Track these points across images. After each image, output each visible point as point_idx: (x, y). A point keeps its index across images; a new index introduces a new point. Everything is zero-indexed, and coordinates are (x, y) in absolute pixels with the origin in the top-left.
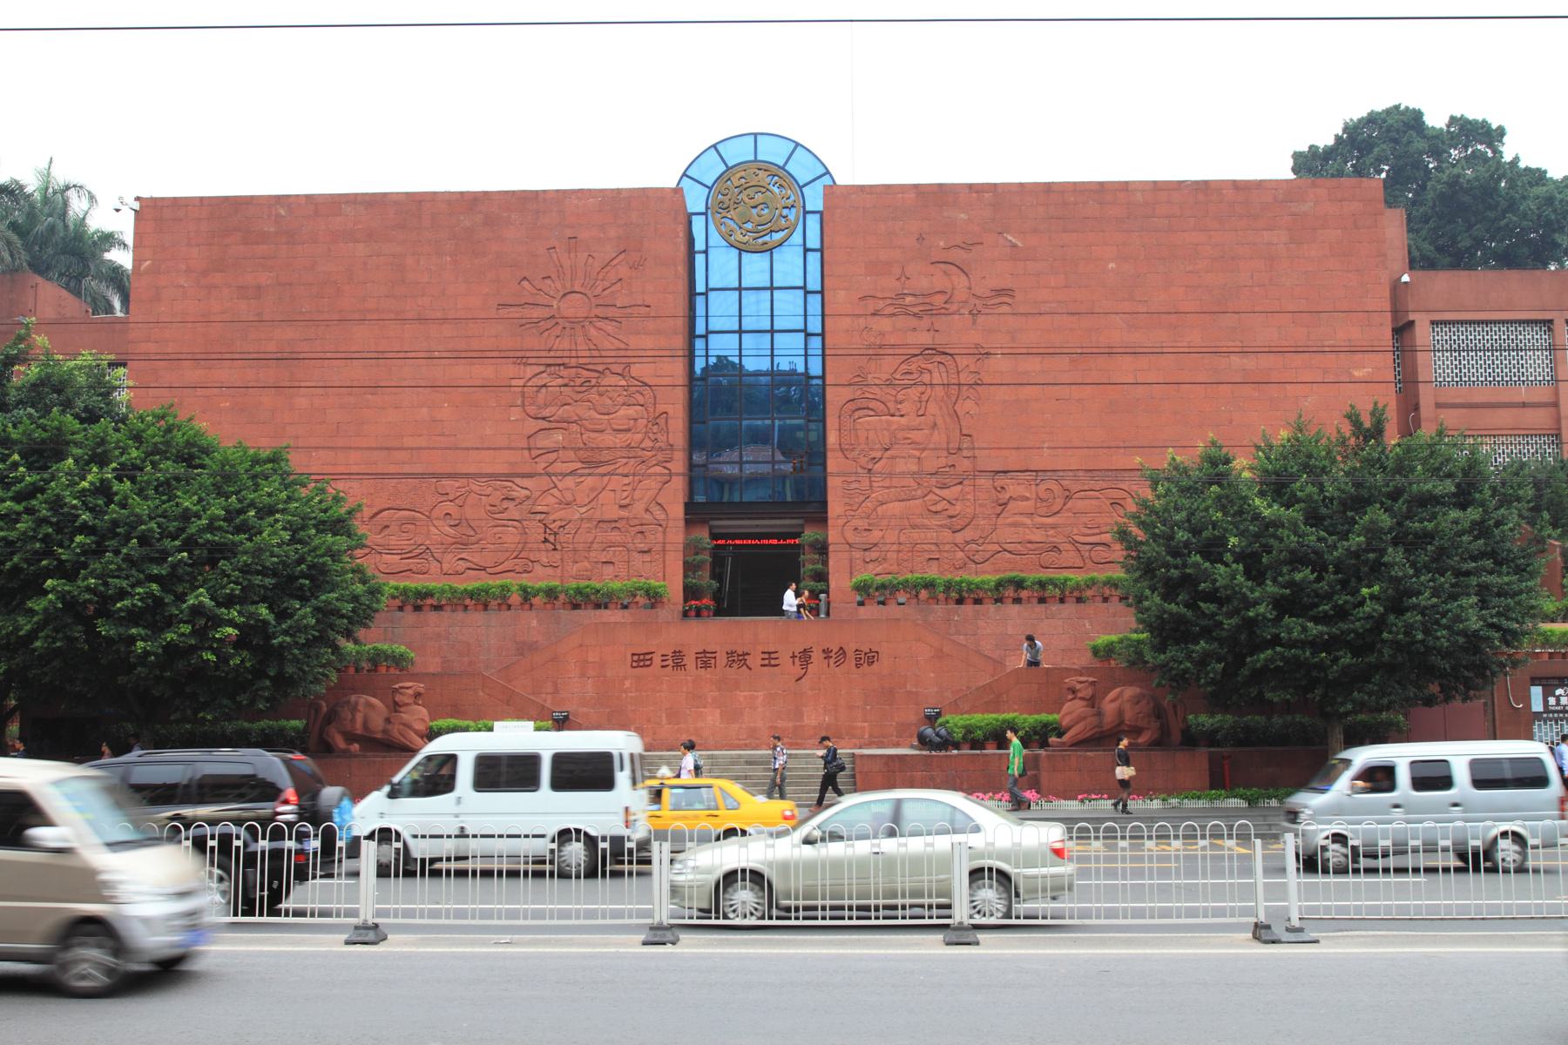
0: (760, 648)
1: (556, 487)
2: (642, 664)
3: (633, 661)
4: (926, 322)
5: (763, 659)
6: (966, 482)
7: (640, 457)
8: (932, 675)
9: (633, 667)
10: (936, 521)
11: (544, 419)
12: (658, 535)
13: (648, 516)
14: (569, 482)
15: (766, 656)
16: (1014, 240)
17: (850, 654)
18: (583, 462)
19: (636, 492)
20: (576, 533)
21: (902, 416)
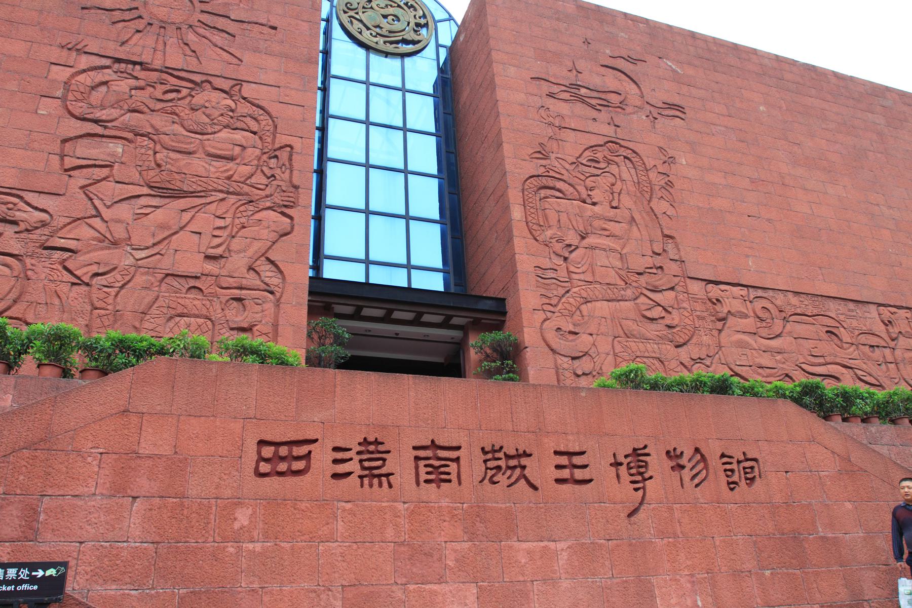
0: (551, 444)
1: (99, 215)
2: (283, 467)
4: (604, 115)
5: (558, 467)
6: (678, 288)
7: (247, 194)
8: (849, 505)
10: (652, 330)
11: (96, 121)
12: (266, 306)
13: (252, 280)
14: (124, 211)
15: (564, 460)
16: (674, 67)
17: (715, 462)
18: (151, 187)
19: (235, 240)
20: (122, 287)
21: (594, 204)
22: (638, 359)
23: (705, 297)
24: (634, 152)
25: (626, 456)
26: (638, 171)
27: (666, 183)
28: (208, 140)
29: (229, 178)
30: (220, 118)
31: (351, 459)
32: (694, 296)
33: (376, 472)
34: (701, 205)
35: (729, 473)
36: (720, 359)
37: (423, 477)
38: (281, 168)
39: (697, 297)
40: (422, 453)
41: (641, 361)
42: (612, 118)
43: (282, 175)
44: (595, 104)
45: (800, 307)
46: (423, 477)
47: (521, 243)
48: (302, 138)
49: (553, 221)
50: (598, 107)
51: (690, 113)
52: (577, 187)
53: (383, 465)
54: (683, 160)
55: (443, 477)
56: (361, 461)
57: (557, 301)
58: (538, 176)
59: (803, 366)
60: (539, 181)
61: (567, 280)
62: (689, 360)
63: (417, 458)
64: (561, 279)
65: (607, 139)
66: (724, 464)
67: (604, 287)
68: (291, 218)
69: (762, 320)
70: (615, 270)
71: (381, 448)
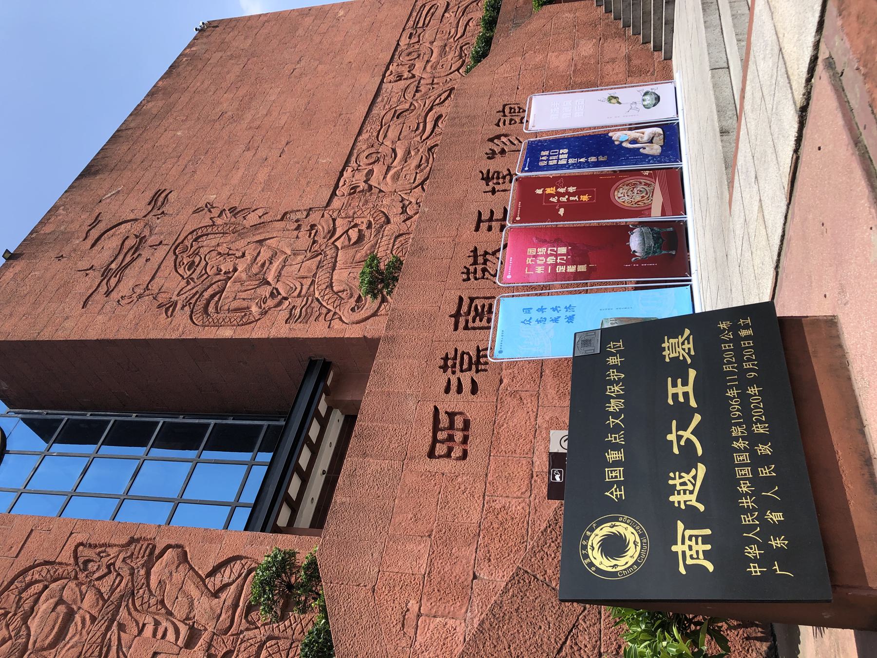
2: (458, 436)
3: (448, 455)
4: (145, 253)
5: (490, 229)
6: (335, 215)
9: (465, 455)
21: (235, 270)
22: (394, 252)
23: (348, 197)
24: (193, 232)
25: (488, 185)
26: (212, 232)
27: (230, 213)
28: (35, 642)
29: (93, 619)
30: (11, 628)
31: (459, 379)
32: (344, 206)
33: (474, 360)
34: (260, 189)
35: (513, 122)
36: (406, 193)
37: (484, 323)
38: (102, 557)
39: (345, 203)
40: (462, 324)
41: (395, 251)
42: (151, 246)
43: (112, 556)
44: (132, 258)
45: (372, 133)
46: (484, 323)
47: (258, 332)
48: (71, 533)
49: (245, 304)
50: (135, 256)
51: (167, 186)
52: (213, 282)
53: (468, 354)
54: (212, 196)
55: (486, 309)
56: (462, 371)
57: (324, 308)
58: (192, 312)
59: (424, 137)
60: (198, 312)
61: (305, 299)
62: (402, 216)
63: (466, 328)
64: (304, 303)
65: (171, 253)
66: (504, 124)
67: (321, 270)
68: (169, 547)
69: (378, 160)
70: (306, 261)
71: (451, 355)
